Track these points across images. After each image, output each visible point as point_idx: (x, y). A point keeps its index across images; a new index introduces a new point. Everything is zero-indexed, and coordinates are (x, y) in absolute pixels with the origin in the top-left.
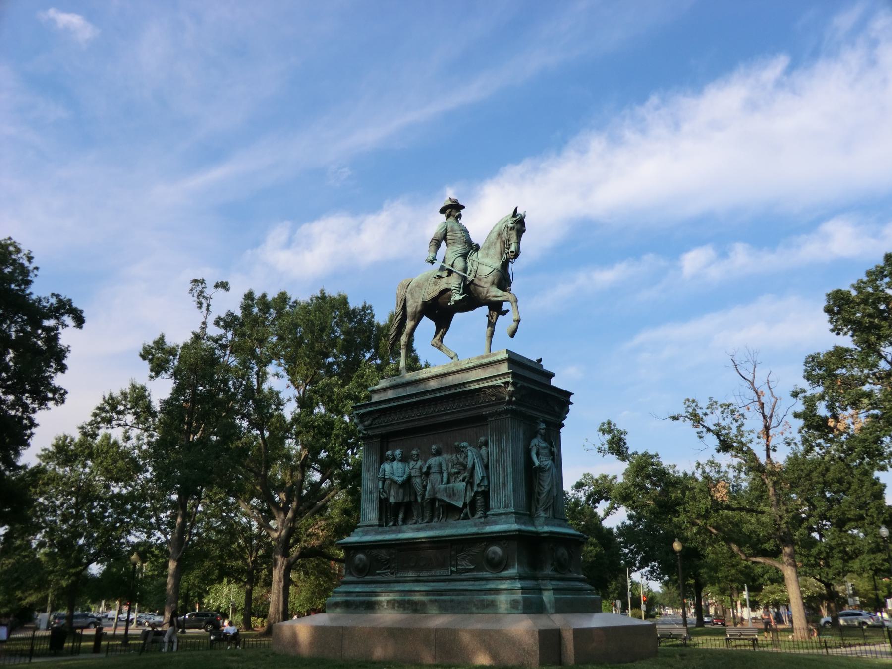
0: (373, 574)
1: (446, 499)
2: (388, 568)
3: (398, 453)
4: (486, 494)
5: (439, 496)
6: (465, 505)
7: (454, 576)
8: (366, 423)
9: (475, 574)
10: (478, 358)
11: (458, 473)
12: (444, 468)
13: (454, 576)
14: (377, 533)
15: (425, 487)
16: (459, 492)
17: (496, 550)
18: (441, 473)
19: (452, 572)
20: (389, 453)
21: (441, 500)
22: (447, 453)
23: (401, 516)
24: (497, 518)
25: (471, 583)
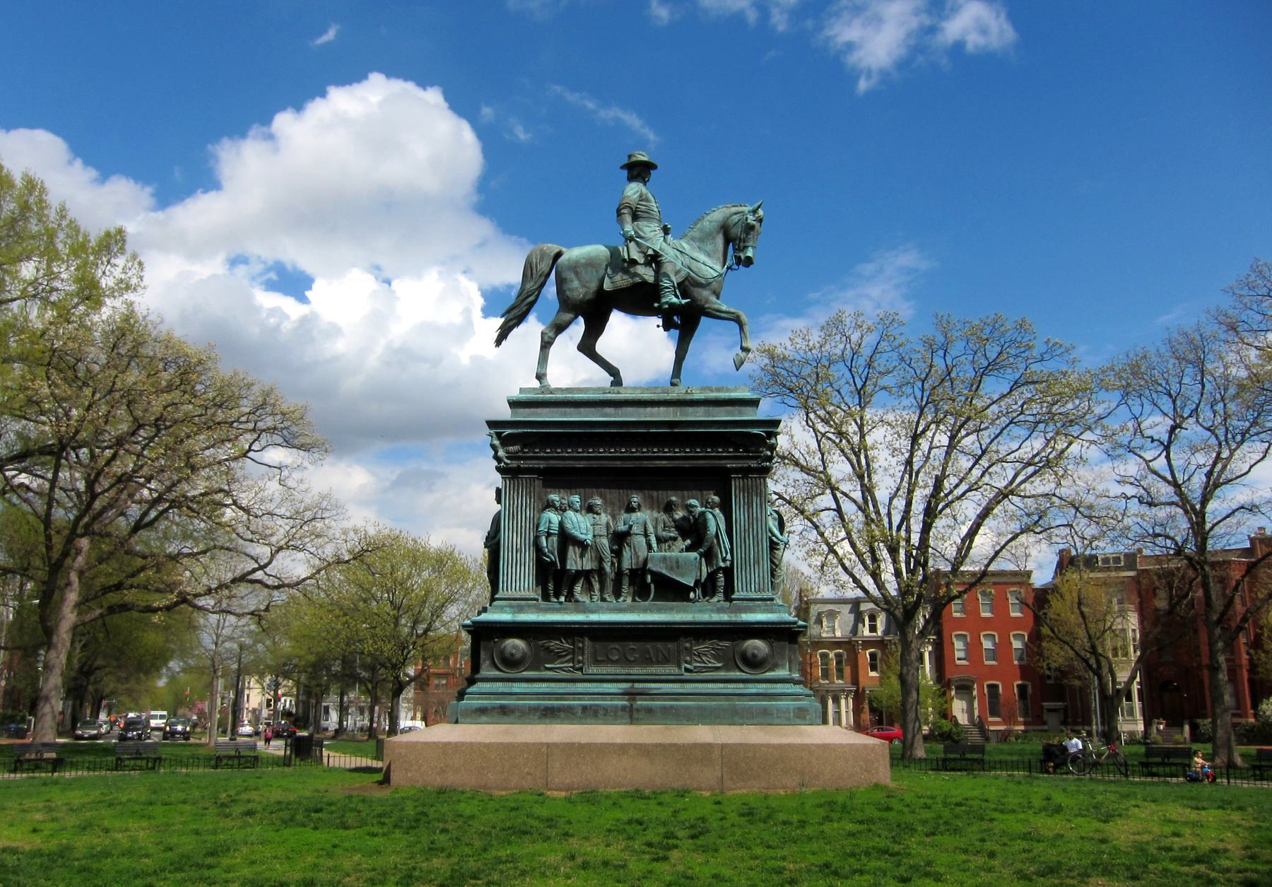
0: (537, 669)
1: (664, 571)
2: (567, 661)
3: (576, 499)
4: (729, 572)
5: (650, 566)
6: (697, 582)
7: (688, 676)
8: (511, 448)
9: (722, 674)
10: (703, 389)
11: (675, 539)
12: (651, 529)
13: (688, 676)
14: (539, 610)
15: (618, 554)
16: (683, 562)
17: (758, 646)
18: (646, 535)
19: (687, 670)
20: (554, 497)
21: (653, 573)
22: (652, 508)
23: (578, 588)
24: (751, 604)
25: (741, 685)
